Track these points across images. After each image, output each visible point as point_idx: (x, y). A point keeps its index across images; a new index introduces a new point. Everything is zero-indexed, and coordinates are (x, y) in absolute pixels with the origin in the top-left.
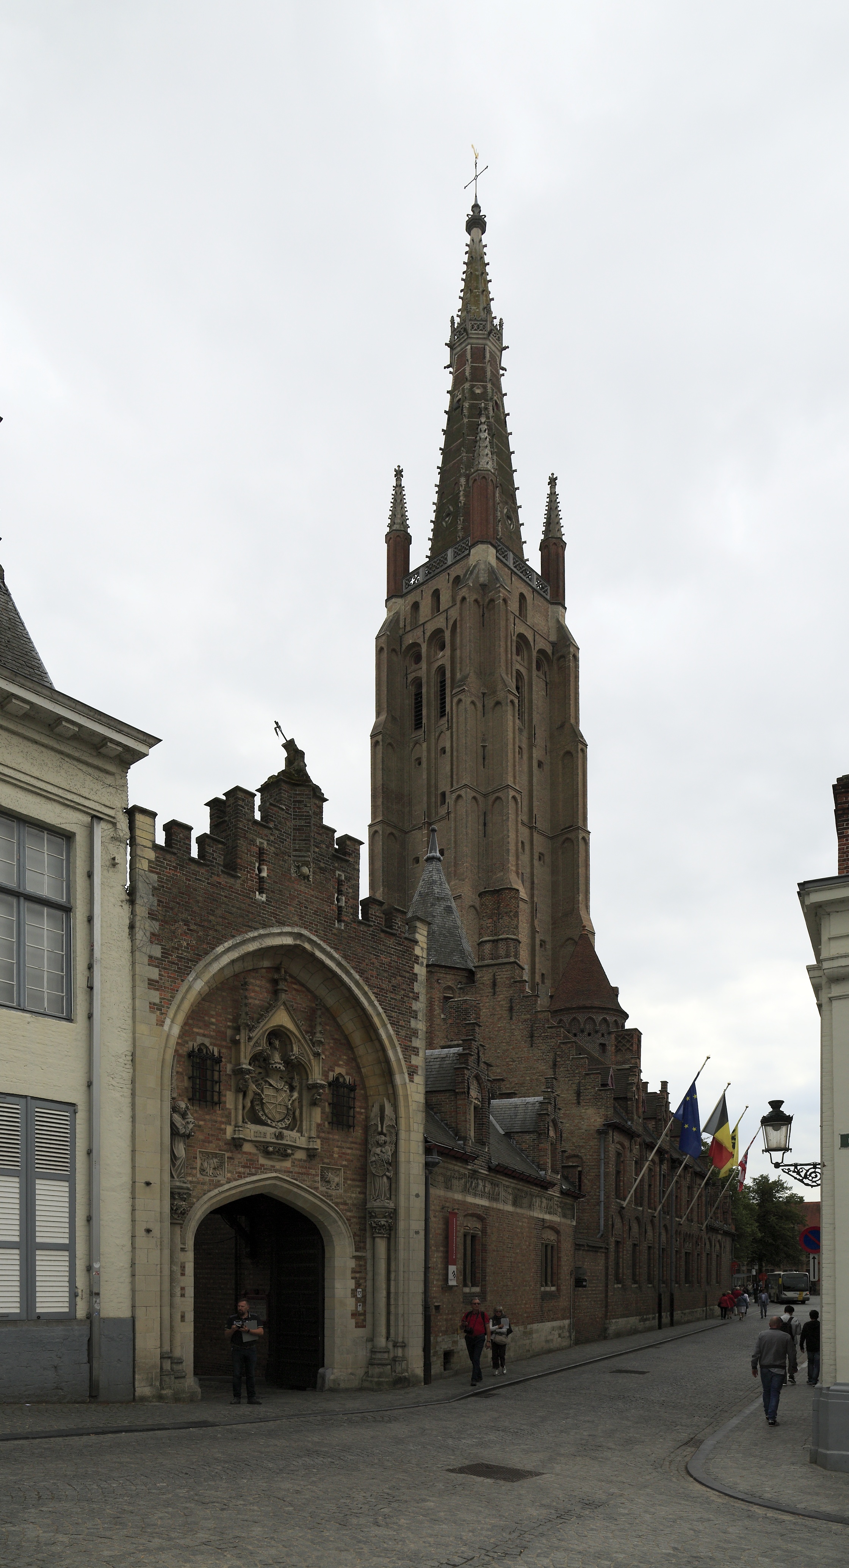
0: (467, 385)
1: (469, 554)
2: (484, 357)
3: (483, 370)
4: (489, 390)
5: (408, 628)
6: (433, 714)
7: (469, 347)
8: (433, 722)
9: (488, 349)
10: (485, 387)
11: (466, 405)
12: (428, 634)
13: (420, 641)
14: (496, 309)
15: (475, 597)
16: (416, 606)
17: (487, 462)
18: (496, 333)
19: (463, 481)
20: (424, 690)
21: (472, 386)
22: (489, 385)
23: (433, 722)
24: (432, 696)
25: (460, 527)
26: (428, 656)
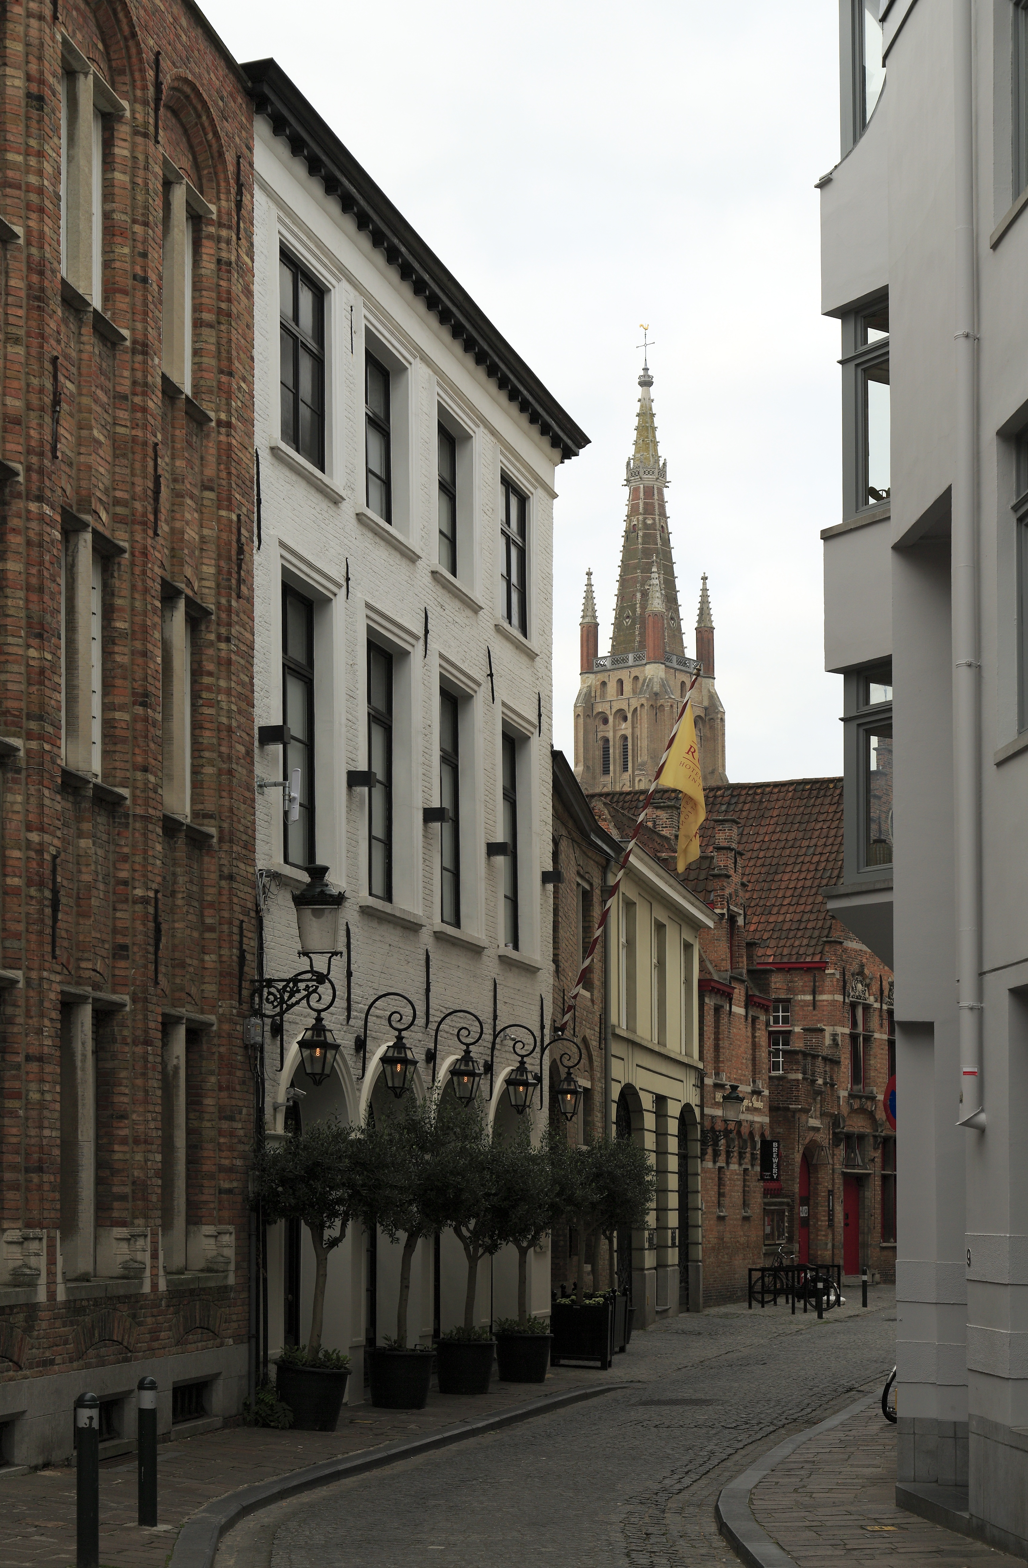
0: (641, 518)
1: (646, 664)
2: (653, 495)
3: (653, 504)
4: (657, 521)
5: (598, 700)
6: (618, 769)
7: (642, 486)
8: (618, 775)
9: (655, 487)
10: (654, 519)
11: (640, 534)
12: (614, 710)
13: (608, 712)
14: (663, 451)
15: (650, 703)
16: (604, 684)
17: (657, 604)
18: (662, 472)
19: (639, 595)
20: (611, 751)
21: (645, 519)
22: (657, 517)
23: (618, 775)
24: (617, 757)
25: (637, 633)
26: (614, 726)
